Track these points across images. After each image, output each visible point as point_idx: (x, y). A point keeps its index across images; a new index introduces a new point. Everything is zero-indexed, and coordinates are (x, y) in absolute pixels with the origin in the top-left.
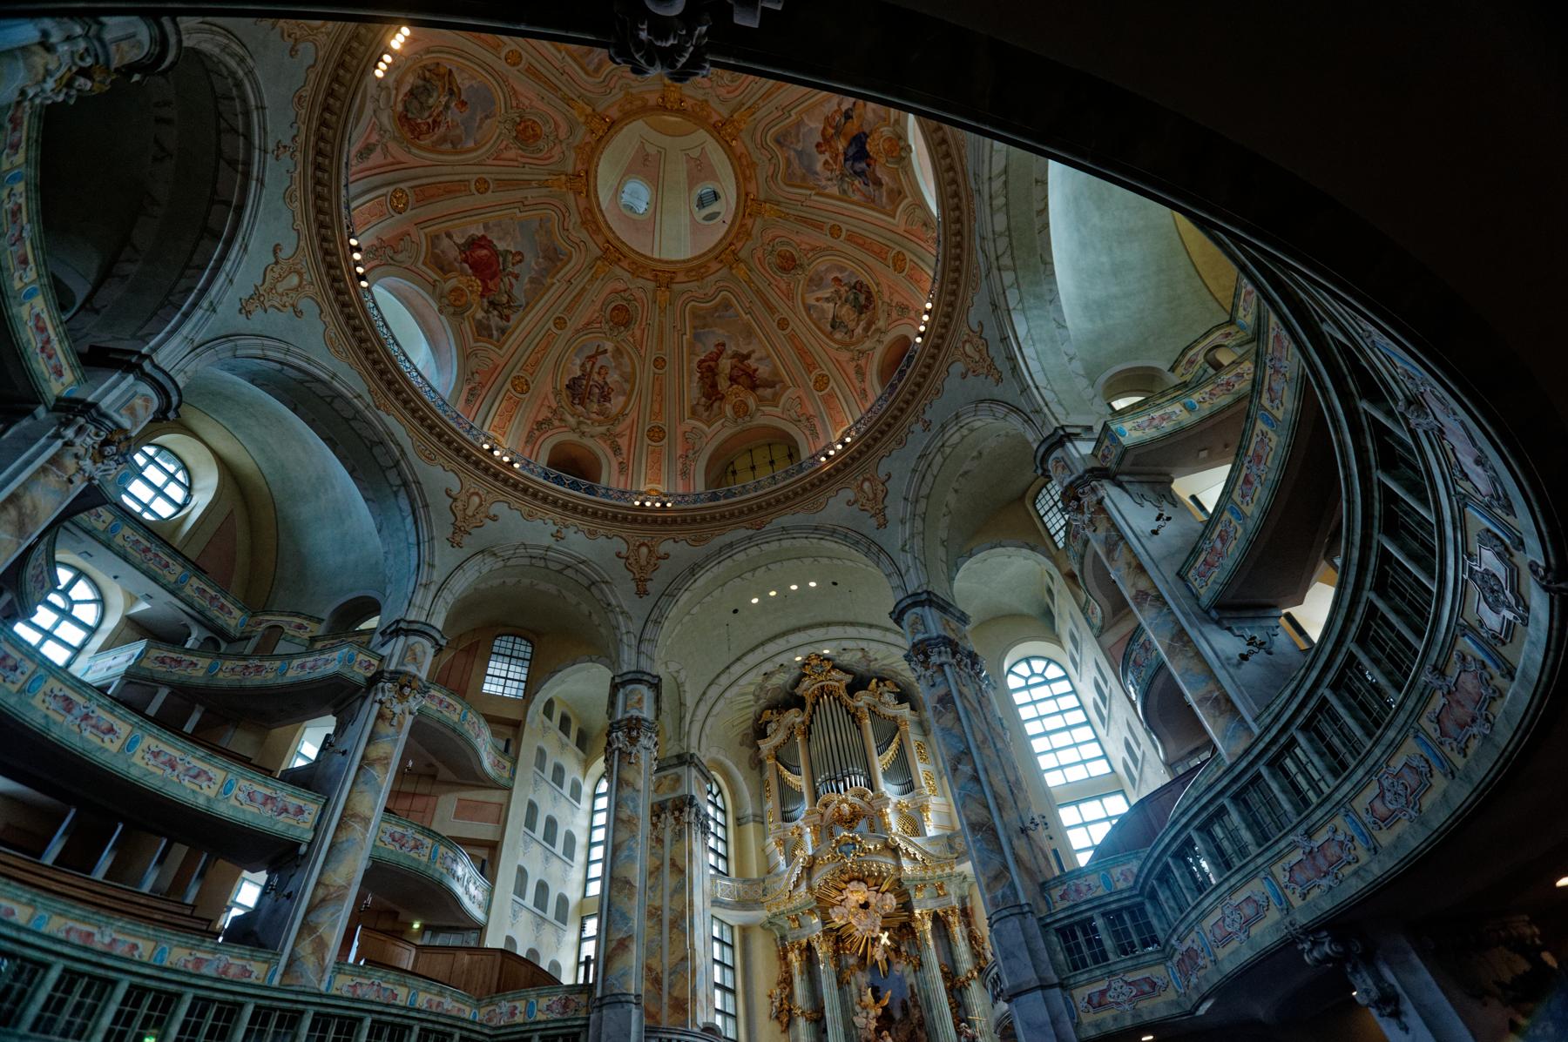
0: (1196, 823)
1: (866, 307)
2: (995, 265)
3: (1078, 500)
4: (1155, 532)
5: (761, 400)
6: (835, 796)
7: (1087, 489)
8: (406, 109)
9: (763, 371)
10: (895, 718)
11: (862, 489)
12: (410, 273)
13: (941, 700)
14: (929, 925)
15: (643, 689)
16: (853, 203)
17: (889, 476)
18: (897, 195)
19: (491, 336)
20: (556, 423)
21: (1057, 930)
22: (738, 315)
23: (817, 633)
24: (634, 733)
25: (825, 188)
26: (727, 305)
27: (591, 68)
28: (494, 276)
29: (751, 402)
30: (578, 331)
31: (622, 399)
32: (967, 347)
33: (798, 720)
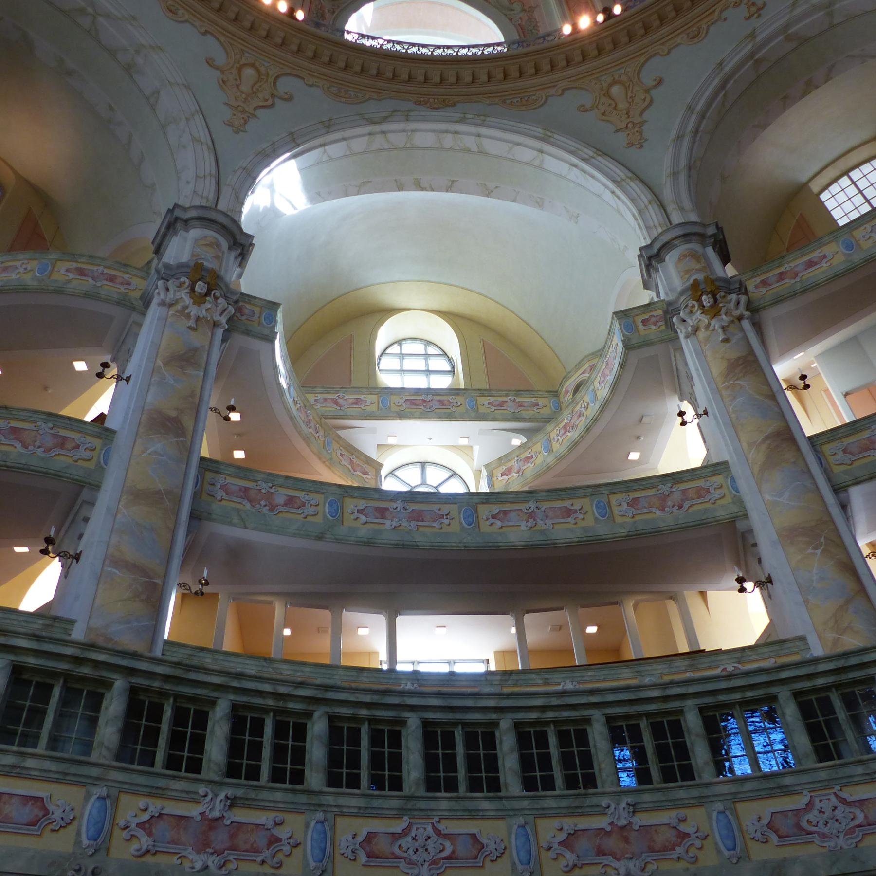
0: (31, 661)
2: (377, 128)
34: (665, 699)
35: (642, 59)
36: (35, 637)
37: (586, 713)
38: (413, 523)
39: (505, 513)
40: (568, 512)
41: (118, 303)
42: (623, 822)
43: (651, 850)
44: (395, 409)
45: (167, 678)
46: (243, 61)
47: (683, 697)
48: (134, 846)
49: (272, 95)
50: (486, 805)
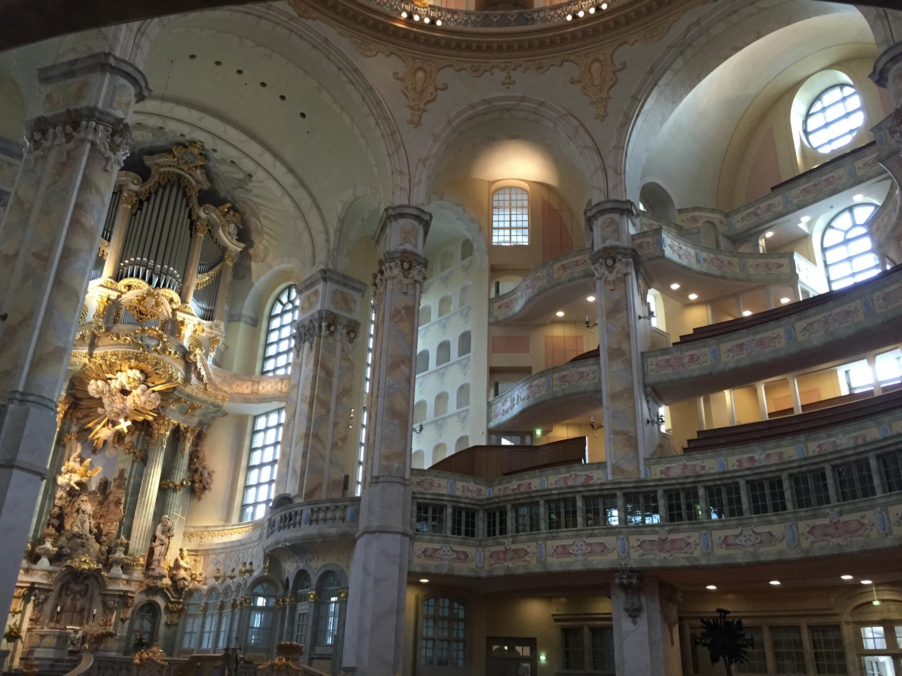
0: (587, 494)
3: (614, 262)
4: (640, 318)
6: (145, 286)
7: (624, 260)
10: (224, 249)
11: (414, 74)
13: (406, 308)
14: (168, 433)
15: (132, 90)
17: (445, 88)
21: (418, 504)
23: (233, 134)
24: (118, 140)
32: (596, 66)
33: (135, 188)
34: (858, 454)
36: (583, 486)
37: (822, 465)
38: (759, 349)
39: (810, 324)
40: (848, 313)
41: (585, 277)
42: (835, 521)
43: (848, 532)
44: (795, 201)
45: (634, 487)
46: (589, 61)
47: (866, 452)
48: (638, 553)
49: (614, 73)
50: (774, 518)
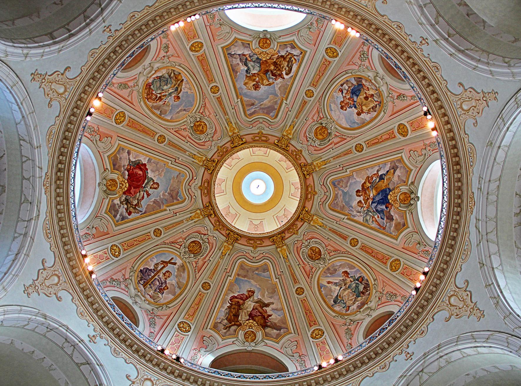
1: (363, 293)
5: (267, 335)
8: (153, 82)
9: (275, 318)
12: (99, 154)
16: (372, 228)
18: (401, 226)
19: (115, 216)
20: (123, 286)
22: (270, 277)
25: (354, 216)
26: (265, 269)
27: (248, 112)
28: (138, 187)
29: (260, 335)
30: (165, 243)
31: (171, 297)
35: (449, 93)
